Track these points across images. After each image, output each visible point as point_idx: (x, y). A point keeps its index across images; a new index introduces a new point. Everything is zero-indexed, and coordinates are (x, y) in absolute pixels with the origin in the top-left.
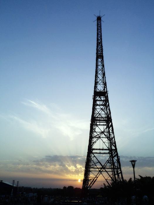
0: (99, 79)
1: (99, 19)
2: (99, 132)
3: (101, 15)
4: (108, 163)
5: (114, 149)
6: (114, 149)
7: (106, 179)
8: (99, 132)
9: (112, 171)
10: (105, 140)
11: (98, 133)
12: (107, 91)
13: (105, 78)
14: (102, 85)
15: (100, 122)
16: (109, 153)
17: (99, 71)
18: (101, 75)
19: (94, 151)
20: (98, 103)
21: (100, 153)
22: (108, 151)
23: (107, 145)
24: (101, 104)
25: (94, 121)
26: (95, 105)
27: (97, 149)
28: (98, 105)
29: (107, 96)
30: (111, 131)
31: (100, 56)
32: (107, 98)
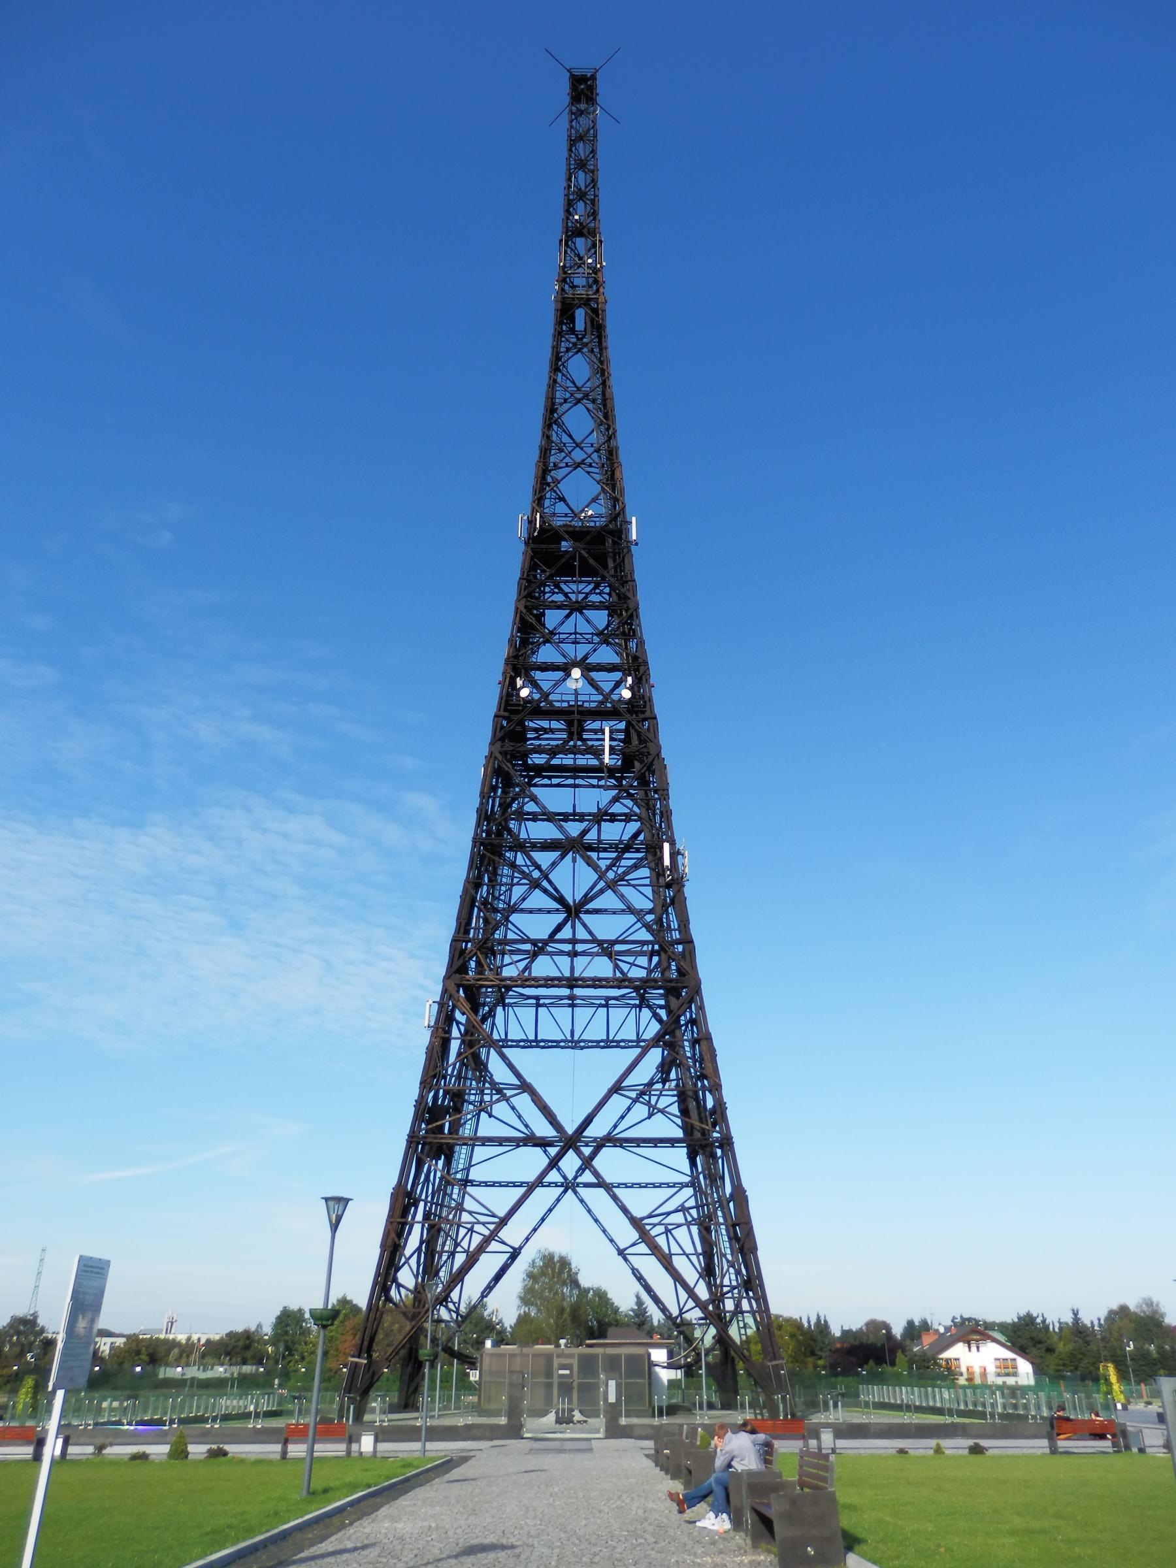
1: (583, 89)
25: (513, 762)
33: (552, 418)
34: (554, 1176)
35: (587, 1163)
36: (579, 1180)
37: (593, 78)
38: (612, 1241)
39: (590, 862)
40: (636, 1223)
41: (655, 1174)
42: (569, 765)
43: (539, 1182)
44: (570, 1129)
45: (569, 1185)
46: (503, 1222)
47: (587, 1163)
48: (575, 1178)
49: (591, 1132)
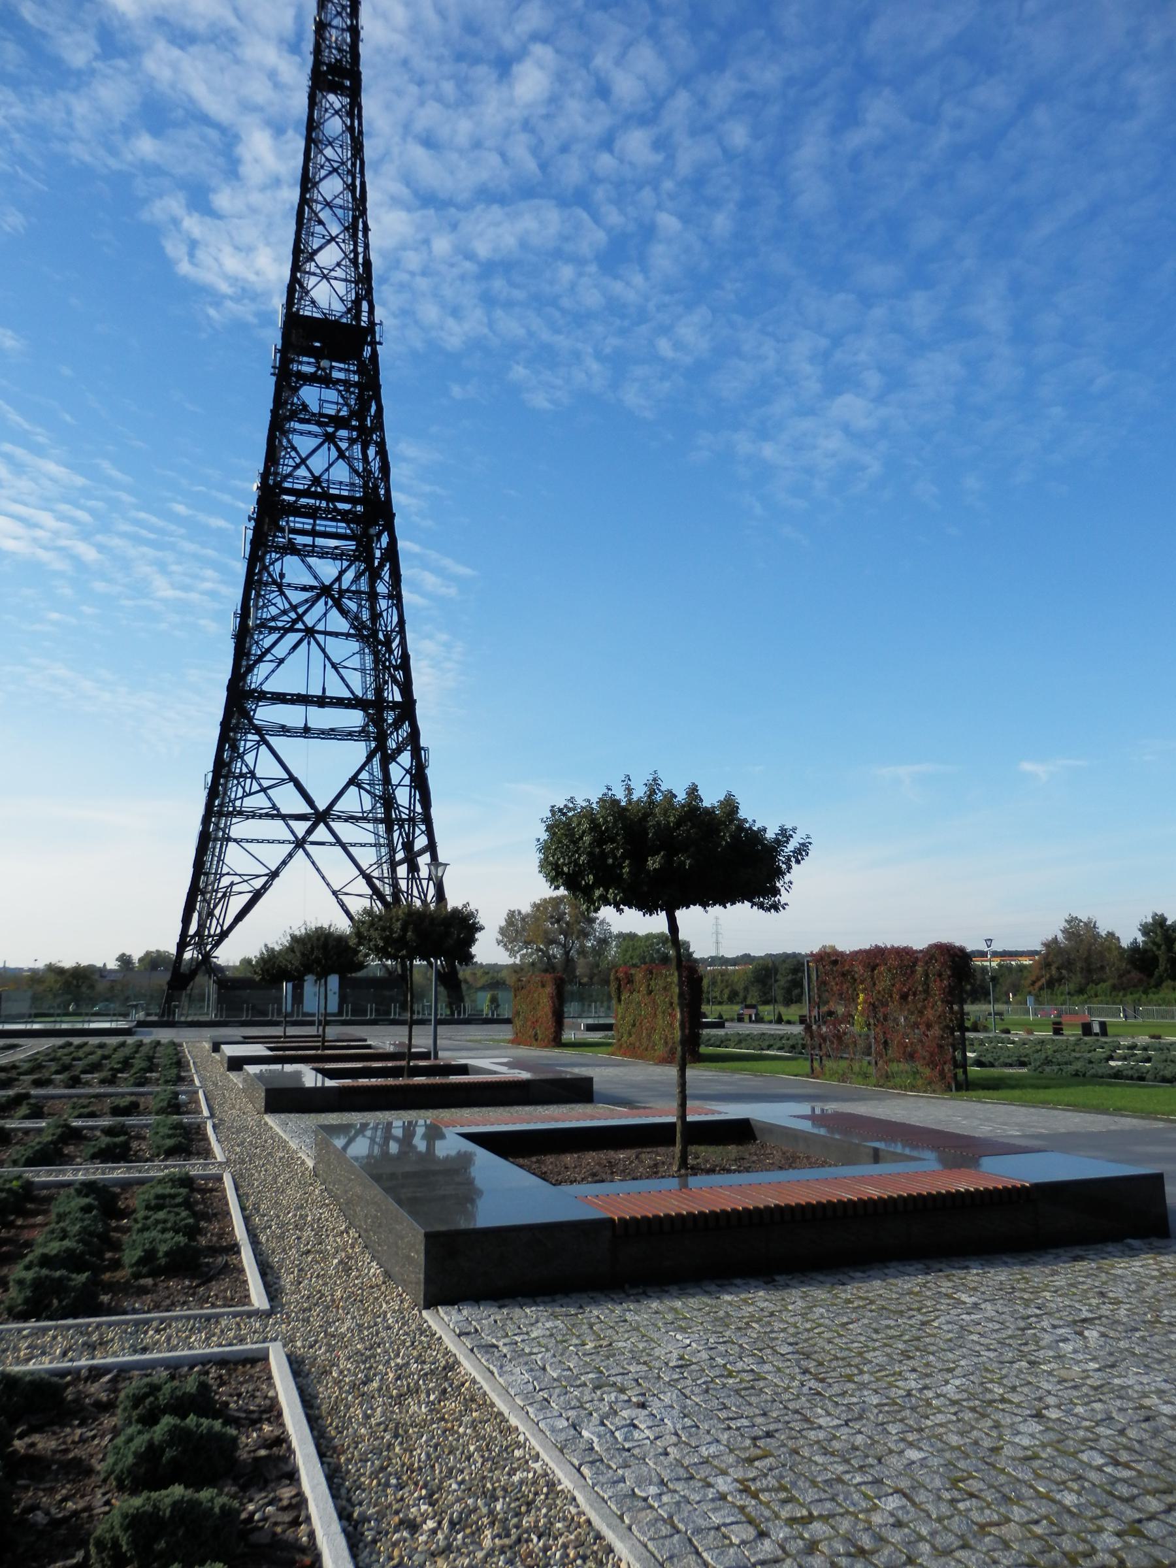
2: (304, 589)
4: (353, 789)
5: (398, 698)
6: (398, 698)
7: (334, 893)
8: (304, 589)
9: (377, 845)
10: (345, 650)
12: (372, 324)
13: (366, 235)
14: (341, 287)
15: (314, 533)
16: (360, 734)
17: (323, 173)
18: (339, 212)
19: (265, 714)
21: (306, 732)
24: (330, 410)
27: (280, 698)
29: (374, 355)
30: (382, 588)
31: (336, 68)
36: (312, 838)
38: (328, 884)
44: (322, 806)
48: (304, 837)
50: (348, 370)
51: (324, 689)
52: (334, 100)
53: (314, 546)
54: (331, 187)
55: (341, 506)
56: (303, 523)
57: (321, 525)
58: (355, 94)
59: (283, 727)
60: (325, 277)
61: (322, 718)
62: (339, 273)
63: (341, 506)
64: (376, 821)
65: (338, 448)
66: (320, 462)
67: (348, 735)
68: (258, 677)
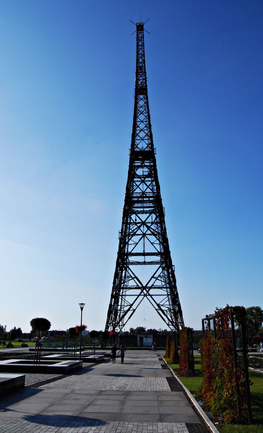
0: (138, 129)
1: (140, 28)
3: (143, 21)
11: (138, 225)
14: (147, 141)
19: (131, 259)
20: (139, 172)
21: (145, 263)
22: (158, 258)
23: (158, 247)
25: (130, 203)
26: (132, 175)
28: (139, 177)
32: (154, 161)
33: (135, 117)
34: (142, 294)
35: (148, 292)
37: (143, 26)
39: (147, 227)
40: (158, 305)
41: (162, 297)
42: (143, 204)
43: (140, 295)
44: (144, 285)
45: (145, 295)
46: (132, 305)
47: (148, 292)
49: (148, 286)
50: (150, 162)
51: (144, 251)
52: (142, 96)
53: (144, 211)
54: (142, 117)
55: (151, 199)
56: (140, 205)
57: (145, 205)
58: (146, 94)
59: (138, 262)
60: (142, 140)
61: (149, 259)
62: (146, 138)
63: (151, 199)
64: (167, 288)
65: (146, 184)
66: (141, 188)
67: (156, 263)
68: (130, 248)
